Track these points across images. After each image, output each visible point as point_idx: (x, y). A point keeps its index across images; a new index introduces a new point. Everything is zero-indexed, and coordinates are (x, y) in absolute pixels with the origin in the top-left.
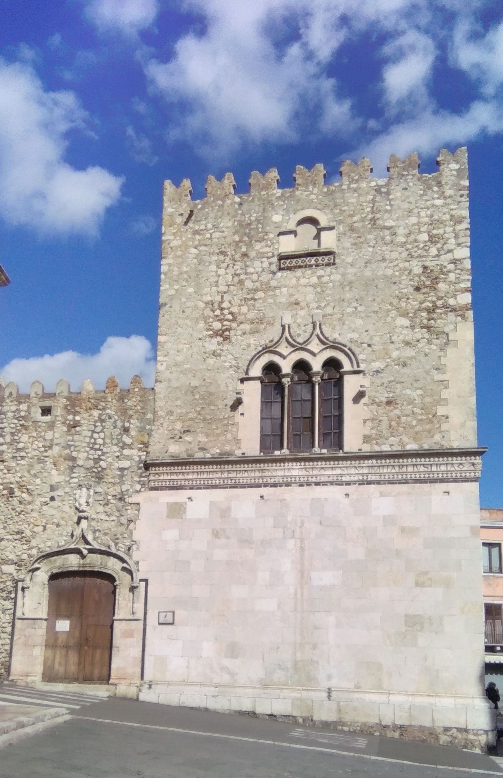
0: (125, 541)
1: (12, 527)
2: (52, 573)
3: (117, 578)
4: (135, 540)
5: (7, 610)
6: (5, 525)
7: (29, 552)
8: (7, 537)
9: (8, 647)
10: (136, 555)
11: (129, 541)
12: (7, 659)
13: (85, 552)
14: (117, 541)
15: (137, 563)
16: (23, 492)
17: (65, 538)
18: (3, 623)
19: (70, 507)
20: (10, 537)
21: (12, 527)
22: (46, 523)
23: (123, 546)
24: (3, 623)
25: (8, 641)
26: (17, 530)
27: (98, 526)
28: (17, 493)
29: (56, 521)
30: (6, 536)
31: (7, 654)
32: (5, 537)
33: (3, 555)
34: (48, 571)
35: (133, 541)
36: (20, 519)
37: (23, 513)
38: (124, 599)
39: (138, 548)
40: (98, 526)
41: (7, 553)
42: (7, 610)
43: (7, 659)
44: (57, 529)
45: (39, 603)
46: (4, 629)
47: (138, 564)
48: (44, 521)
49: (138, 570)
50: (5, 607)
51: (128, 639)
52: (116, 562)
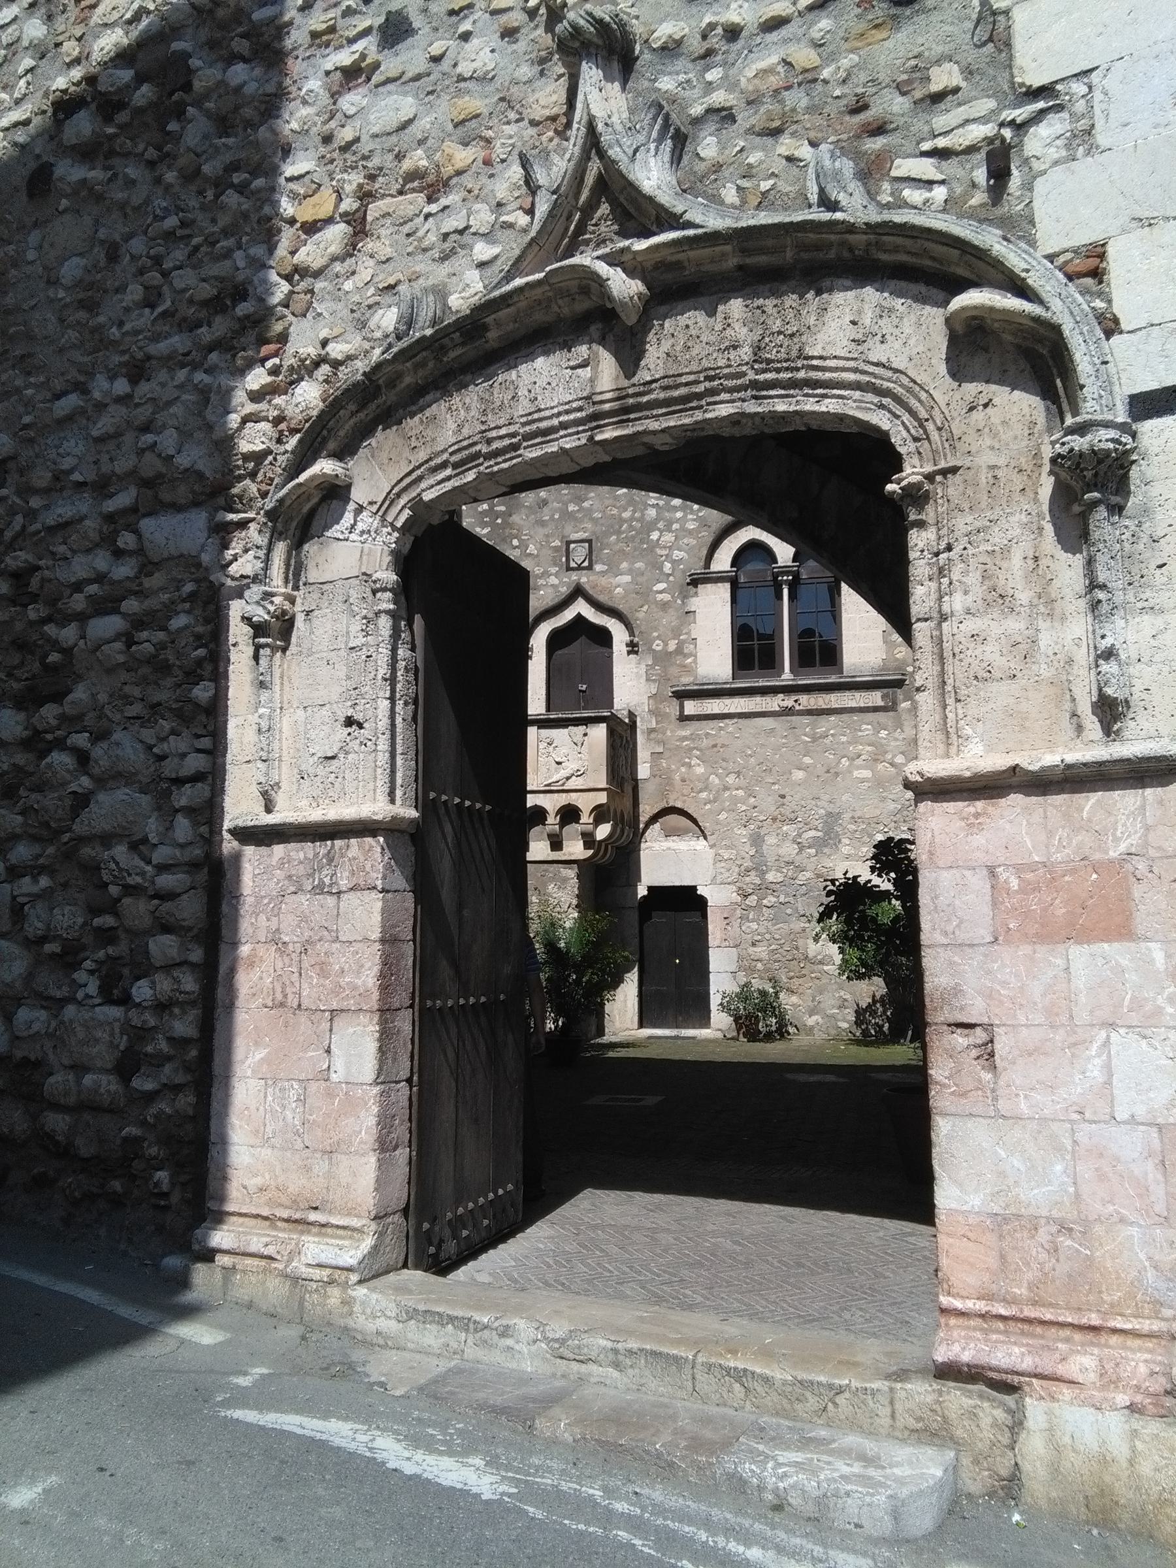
0: (941, 121)
1: (185, 279)
2: (417, 505)
3: (899, 439)
4: (1036, 81)
5: (179, 782)
6: (154, 277)
7: (279, 400)
8: (161, 348)
9: (184, 1026)
10: (1064, 205)
11: (987, 105)
12: (186, 1101)
13: (623, 286)
14: (875, 144)
15: (1090, 267)
16: (233, 58)
17: (482, 250)
18: (162, 868)
19: (509, 33)
20: (177, 342)
21: (185, 279)
22: (365, 196)
23: (926, 168)
24: (162, 868)
25: (190, 983)
26: (207, 291)
27: (709, 87)
28: (206, 75)
29: (418, 159)
30: (156, 338)
31: (188, 1069)
32: (153, 349)
33: (148, 456)
34: (391, 499)
35: (1034, 94)
36: (224, 220)
37: (237, 178)
38: (999, 599)
39: (1083, 138)
40: (709, 87)
41: (168, 441)
42: (179, 782)
43: (186, 1101)
44: (433, 208)
45: (349, 722)
46: (167, 906)
47: (1097, 274)
48: (355, 179)
49: (1110, 326)
50: (169, 768)
51: (1082, 958)
52: (884, 312)
